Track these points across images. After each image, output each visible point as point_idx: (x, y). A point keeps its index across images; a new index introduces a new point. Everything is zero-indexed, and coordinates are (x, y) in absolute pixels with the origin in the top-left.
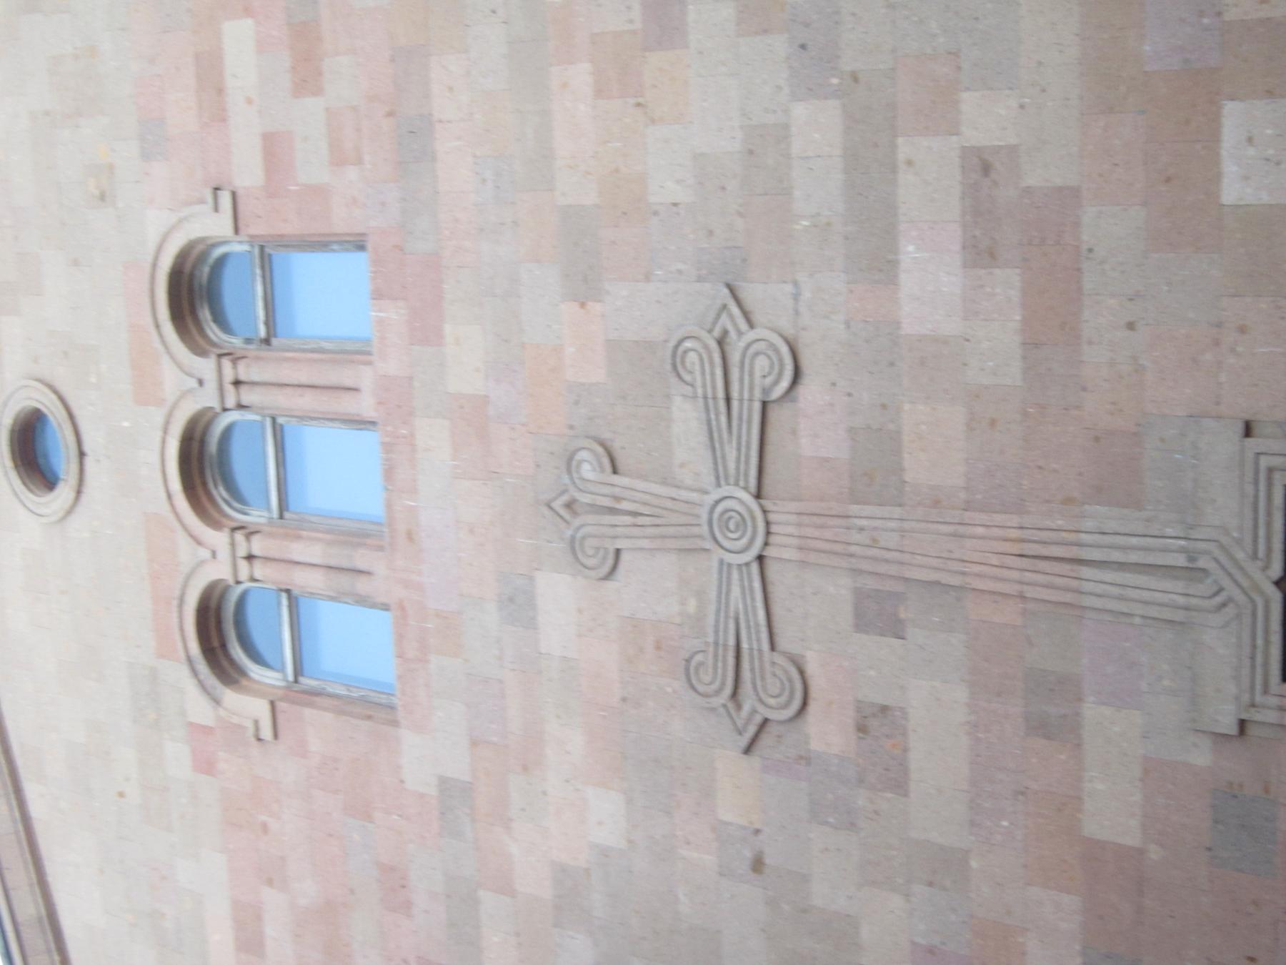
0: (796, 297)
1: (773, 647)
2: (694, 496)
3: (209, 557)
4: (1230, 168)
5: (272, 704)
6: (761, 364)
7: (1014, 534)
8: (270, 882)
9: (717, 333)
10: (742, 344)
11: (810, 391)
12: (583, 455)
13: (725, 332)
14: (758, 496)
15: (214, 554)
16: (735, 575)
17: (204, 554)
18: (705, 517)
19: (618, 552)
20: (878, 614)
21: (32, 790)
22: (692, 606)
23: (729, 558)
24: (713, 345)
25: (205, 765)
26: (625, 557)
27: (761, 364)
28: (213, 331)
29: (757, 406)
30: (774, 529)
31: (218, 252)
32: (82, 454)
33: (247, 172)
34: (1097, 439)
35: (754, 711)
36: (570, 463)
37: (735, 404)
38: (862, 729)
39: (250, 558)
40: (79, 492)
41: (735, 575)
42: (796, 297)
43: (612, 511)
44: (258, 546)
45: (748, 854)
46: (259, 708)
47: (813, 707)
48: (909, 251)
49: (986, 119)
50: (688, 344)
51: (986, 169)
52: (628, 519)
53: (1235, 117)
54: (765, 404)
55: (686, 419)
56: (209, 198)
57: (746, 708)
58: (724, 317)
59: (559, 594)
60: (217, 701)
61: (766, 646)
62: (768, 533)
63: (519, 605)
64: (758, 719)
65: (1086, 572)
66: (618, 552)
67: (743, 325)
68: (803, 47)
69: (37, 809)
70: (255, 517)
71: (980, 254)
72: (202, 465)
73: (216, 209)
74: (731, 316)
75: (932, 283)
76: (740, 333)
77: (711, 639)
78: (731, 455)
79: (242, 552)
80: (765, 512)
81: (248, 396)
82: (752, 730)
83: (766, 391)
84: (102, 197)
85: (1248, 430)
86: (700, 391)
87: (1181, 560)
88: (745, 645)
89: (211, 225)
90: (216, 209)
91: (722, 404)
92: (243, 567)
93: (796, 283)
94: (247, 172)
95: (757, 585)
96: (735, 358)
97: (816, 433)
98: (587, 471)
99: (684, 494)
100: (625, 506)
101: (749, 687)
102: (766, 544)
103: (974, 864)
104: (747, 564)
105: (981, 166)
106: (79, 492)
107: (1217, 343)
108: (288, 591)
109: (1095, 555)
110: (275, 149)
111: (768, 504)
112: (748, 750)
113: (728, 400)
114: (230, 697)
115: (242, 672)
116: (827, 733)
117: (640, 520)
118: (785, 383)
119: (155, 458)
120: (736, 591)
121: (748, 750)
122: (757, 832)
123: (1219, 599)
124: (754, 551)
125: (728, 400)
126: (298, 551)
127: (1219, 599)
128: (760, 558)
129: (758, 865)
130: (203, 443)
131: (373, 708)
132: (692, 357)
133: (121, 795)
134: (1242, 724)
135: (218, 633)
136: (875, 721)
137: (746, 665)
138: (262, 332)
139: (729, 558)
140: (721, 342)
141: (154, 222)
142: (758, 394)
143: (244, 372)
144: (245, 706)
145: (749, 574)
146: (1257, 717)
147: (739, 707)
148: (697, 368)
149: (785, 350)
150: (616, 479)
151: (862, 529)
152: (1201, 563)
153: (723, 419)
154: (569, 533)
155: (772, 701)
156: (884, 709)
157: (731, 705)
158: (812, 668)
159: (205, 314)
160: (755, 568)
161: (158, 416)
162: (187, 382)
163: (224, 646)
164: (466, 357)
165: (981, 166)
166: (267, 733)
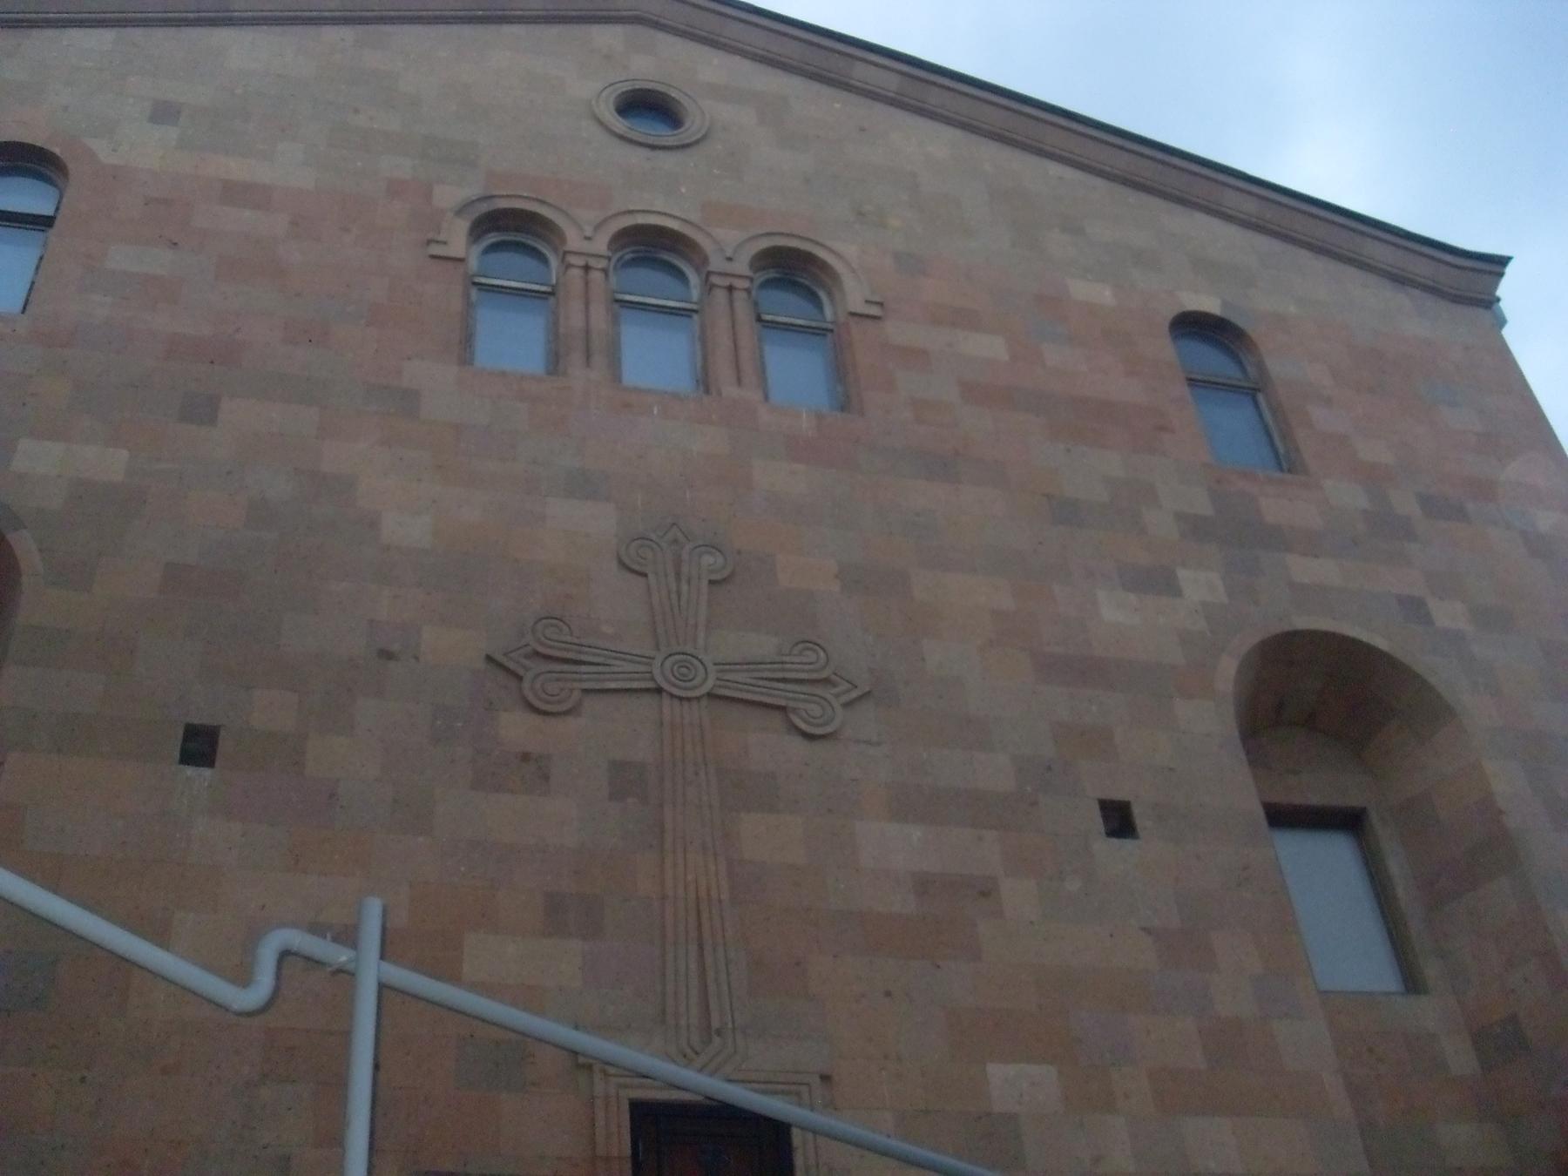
0: (868, 743)
1: (586, 691)
2: (701, 642)
3: (586, 235)
4: (1012, 1070)
5: (461, 260)
6: (815, 710)
7: (714, 894)
9: (833, 677)
10: (828, 696)
11: (797, 746)
12: (720, 560)
13: (834, 685)
14: (711, 696)
15: (588, 238)
16: (642, 668)
17: (589, 232)
18: (689, 649)
19: (645, 575)
20: (626, 780)
21: (347, 33)
22: (606, 629)
23: (657, 663)
24: (824, 675)
25: (396, 189)
26: (640, 579)
27: (815, 710)
28: (761, 277)
29: (783, 703)
30: (686, 704)
31: (822, 295)
32: (653, 147)
33: (897, 332)
34: (798, 964)
35: (527, 669)
36: (714, 547)
37: (781, 686)
38: (526, 757)
39: (587, 268)
40: (622, 137)
41: (642, 668)
42: (868, 743)
43: (678, 575)
44: (596, 276)
45: (395, 647)
47: (536, 720)
48: (916, 833)
50: (822, 654)
51: (985, 894)
52: (674, 587)
53: (1046, 1074)
54: (782, 709)
55: (762, 645)
56: (877, 299)
57: (527, 662)
58: (846, 686)
59: (598, 522)
60: (460, 211)
61: (586, 685)
62: (681, 699)
63: (583, 486)
64: (521, 672)
65: (693, 948)
66: (645, 575)
67: (845, 699)
68: (1049, 768)
69: (332, 34)
70: (613, 279)
71: (924, 885)
72: (651, 246)
73: (867, 302)
74: (848, 691)
75: (895, 848)
76: (837, 696)
77: (583, 641)
78: (740, 677)
79: (592, 262)
80: (698, 699)
81: (720, 296)
82: (511, 665)
83: (794, 710)
84: (860, 214)
85: (825, 1078)
86: (787, 659)
87: (715, 1024)
88: (584, 668)
89: (854, 294)
90: (867, 302)
91: (780, 675)
93: (879, 744)
94: (897, 332)
95: (635, 685)
96: (819, 690)
97: (765, 747)
98: (708, 560)
99: (701, 635)
100: (685, 587)
101: (541, 665)
102: (672, 696)
103: (421, 839)
104: (653, 679)
105: (986, 891)
106: (622, 137)
107: (886, 1057)
108: (552, 294)
109: (709, 960)
110: (916, 357)
111: (704, 702)
112: (489, 659)
113: (784, 680)
114: (462, 227)
116: (515, 728)
117: (674, 596)
118: (803, 726)
119: (659, 205)
121: (489, 659)
122: (417, 658)
123: (689, 1051)
124: (665, 686)
125: (784, 680)
127: (689, 1051)
128: (659, 691)
129: (387, 655)
130: (671, 250)
131: (465, 346)
132: (812, 657)
133: (356, 111)
134: (589, 1067)
135: (511, 227)
136: (534, 770)
137: (566, 667)
138: (769, 317)
139: (657, 663)
140: (826, 681)
141: (850, 250)
142: (791, 704)
143: (740, 296)
144: (457, 239)
145: (644, 679)
146: (597, 1077)
147: (527, 657)
148: (805, 660)
149: (829, 729)
150: (705, 583)
151: (697, 774)
152: (717, 1040)
153: (766, 674)
154: (653, 537)
155: (538, 686)
156: (546, 778)
157: (529, 649)
159: (772, 274)
160: (650, 685)
161: (694, 217)
162: (730, 247)
163: (498, 229)
166: (436, 250)
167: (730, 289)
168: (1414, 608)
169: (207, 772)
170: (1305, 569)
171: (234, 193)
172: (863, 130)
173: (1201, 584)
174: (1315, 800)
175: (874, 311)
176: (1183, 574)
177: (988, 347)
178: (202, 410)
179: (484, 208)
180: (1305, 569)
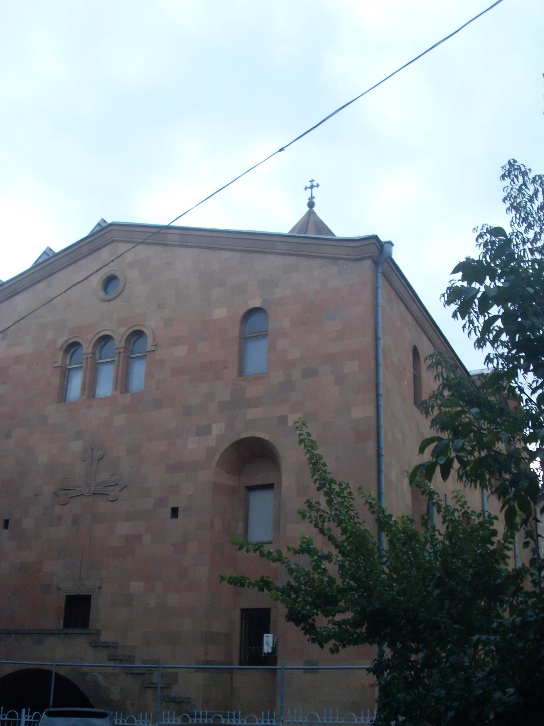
8: (28, 366)
14: (93, 493)
21: (42, 285)
32: (109, 301)
39: (87, 358)
46: (59, 364)
49: (147, 538)
55: (104, 476)
57: (61, 492)
60: (60, 349)
63: (77, 436)
70: (98, 355)
75: (124, 528)
78: (98, 487)
85: (100, 588)
92: (85, 357)
98: (99, 453)
114: (61, 353)
115: (68, 353)
120: (79, 489)
126: (88, 372)
129: (37, 495)
143: (122, 354)
158: (68, 506)
164: (120, 420)
165: (138, 538)
166: (56, 365)
167: (120, 353)
168: (283, 420)
169: (6, 531)
170: (252, 413)
171: (18, 359)
172: (168, 264)
173: (218, 429)
174: (260, 483)
175: (153, 348)
176: (214, 426)
177: (181, 351)
178: (8, 435)
179: (67, 344)
180: (252, 413)
